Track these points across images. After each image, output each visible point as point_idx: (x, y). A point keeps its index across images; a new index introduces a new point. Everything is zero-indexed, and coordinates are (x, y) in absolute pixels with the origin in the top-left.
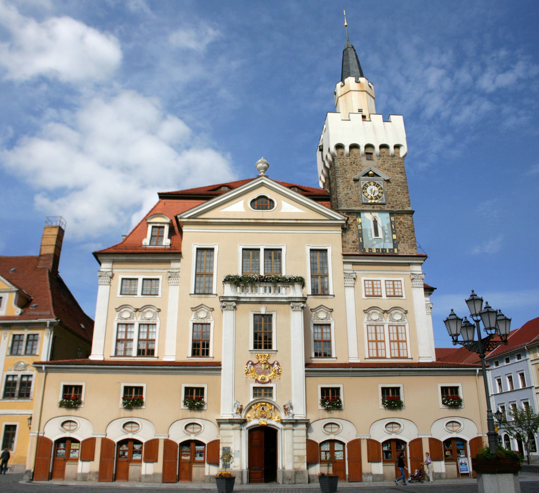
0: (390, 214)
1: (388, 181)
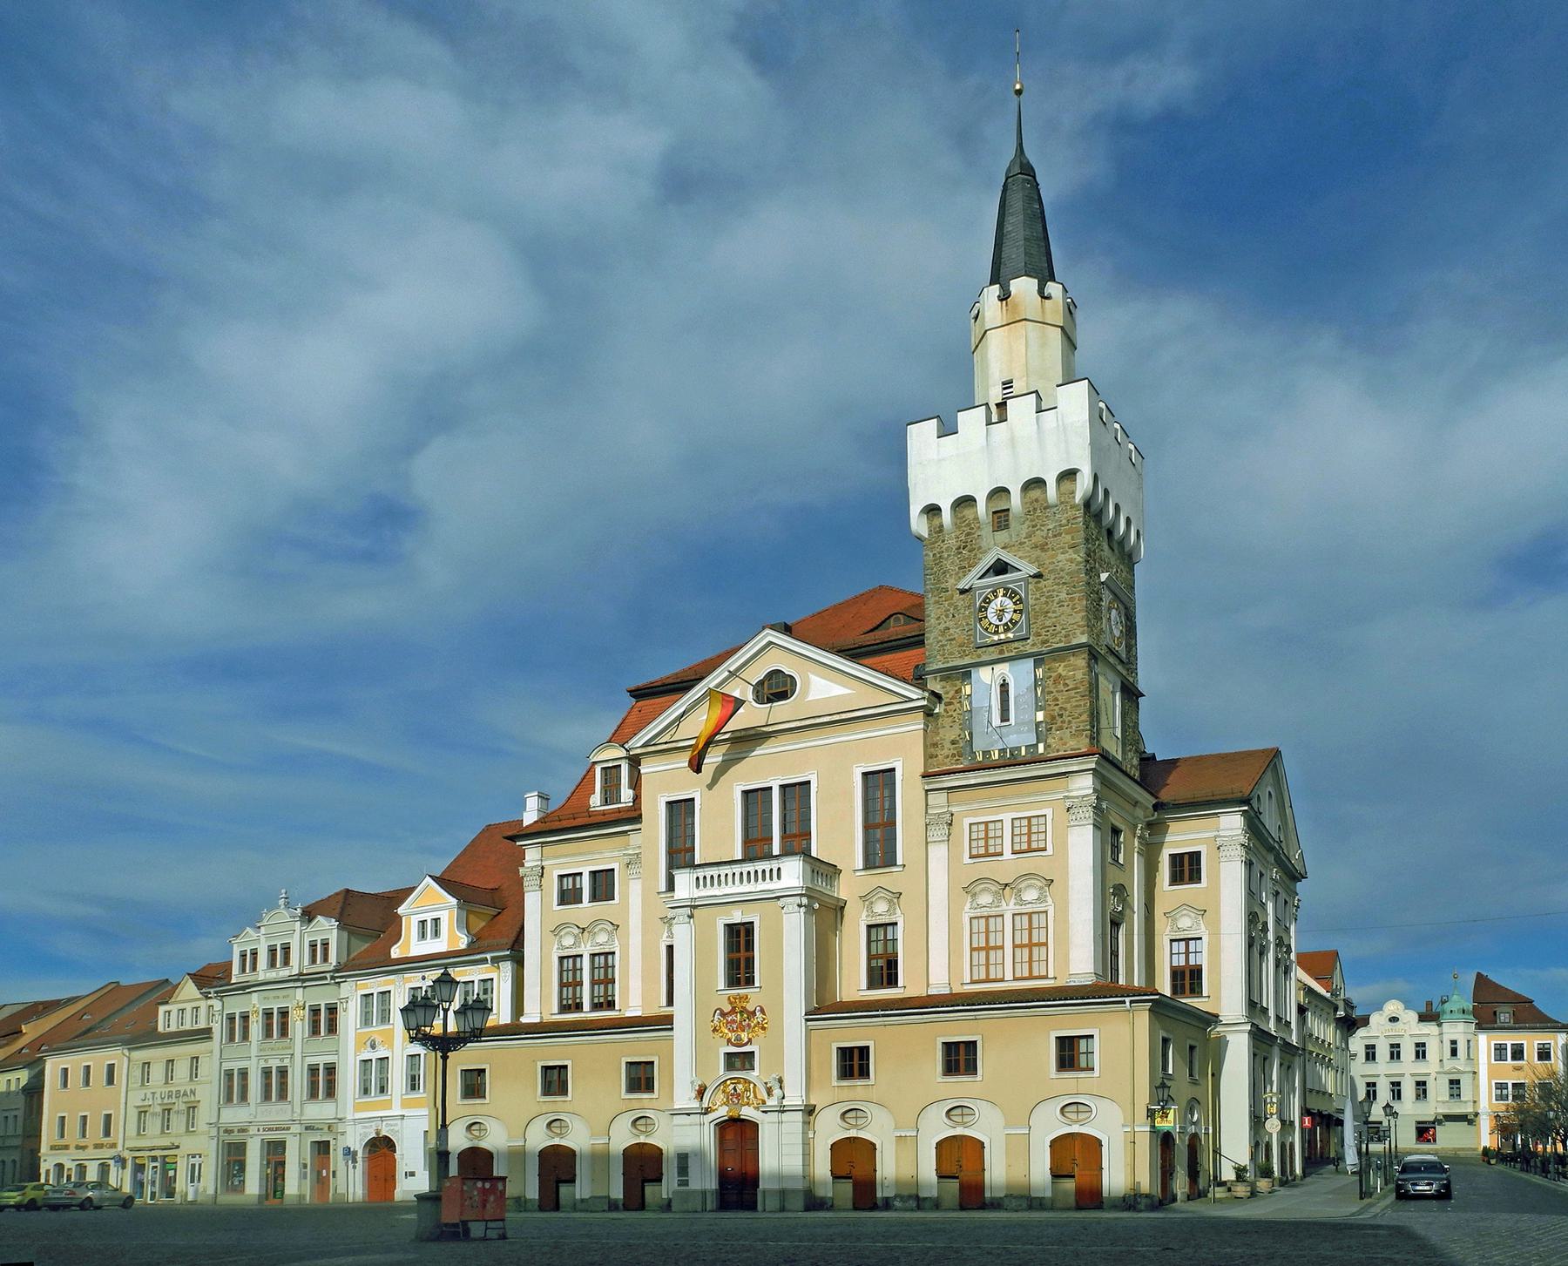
1: (1038, 576)
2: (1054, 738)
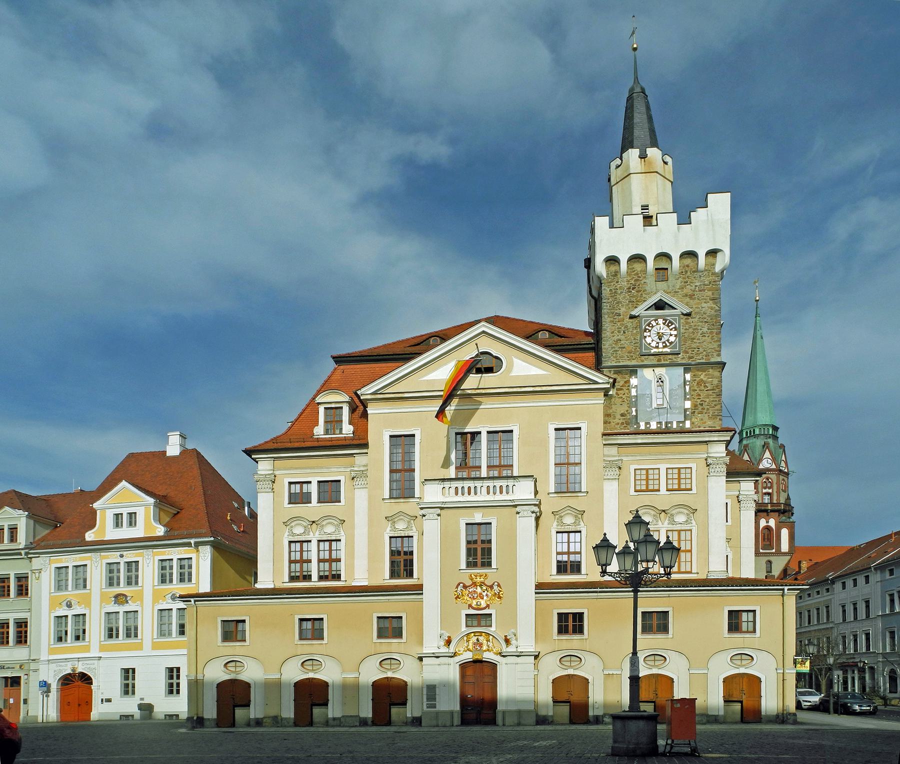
1: (688, 315)
2: (697, 419)
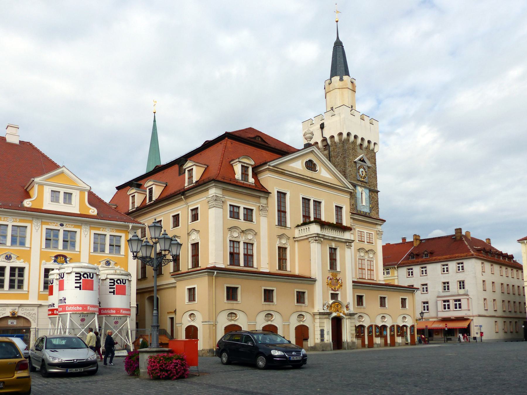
0: (369, 190)
